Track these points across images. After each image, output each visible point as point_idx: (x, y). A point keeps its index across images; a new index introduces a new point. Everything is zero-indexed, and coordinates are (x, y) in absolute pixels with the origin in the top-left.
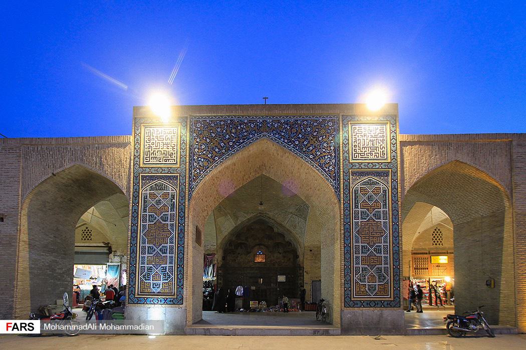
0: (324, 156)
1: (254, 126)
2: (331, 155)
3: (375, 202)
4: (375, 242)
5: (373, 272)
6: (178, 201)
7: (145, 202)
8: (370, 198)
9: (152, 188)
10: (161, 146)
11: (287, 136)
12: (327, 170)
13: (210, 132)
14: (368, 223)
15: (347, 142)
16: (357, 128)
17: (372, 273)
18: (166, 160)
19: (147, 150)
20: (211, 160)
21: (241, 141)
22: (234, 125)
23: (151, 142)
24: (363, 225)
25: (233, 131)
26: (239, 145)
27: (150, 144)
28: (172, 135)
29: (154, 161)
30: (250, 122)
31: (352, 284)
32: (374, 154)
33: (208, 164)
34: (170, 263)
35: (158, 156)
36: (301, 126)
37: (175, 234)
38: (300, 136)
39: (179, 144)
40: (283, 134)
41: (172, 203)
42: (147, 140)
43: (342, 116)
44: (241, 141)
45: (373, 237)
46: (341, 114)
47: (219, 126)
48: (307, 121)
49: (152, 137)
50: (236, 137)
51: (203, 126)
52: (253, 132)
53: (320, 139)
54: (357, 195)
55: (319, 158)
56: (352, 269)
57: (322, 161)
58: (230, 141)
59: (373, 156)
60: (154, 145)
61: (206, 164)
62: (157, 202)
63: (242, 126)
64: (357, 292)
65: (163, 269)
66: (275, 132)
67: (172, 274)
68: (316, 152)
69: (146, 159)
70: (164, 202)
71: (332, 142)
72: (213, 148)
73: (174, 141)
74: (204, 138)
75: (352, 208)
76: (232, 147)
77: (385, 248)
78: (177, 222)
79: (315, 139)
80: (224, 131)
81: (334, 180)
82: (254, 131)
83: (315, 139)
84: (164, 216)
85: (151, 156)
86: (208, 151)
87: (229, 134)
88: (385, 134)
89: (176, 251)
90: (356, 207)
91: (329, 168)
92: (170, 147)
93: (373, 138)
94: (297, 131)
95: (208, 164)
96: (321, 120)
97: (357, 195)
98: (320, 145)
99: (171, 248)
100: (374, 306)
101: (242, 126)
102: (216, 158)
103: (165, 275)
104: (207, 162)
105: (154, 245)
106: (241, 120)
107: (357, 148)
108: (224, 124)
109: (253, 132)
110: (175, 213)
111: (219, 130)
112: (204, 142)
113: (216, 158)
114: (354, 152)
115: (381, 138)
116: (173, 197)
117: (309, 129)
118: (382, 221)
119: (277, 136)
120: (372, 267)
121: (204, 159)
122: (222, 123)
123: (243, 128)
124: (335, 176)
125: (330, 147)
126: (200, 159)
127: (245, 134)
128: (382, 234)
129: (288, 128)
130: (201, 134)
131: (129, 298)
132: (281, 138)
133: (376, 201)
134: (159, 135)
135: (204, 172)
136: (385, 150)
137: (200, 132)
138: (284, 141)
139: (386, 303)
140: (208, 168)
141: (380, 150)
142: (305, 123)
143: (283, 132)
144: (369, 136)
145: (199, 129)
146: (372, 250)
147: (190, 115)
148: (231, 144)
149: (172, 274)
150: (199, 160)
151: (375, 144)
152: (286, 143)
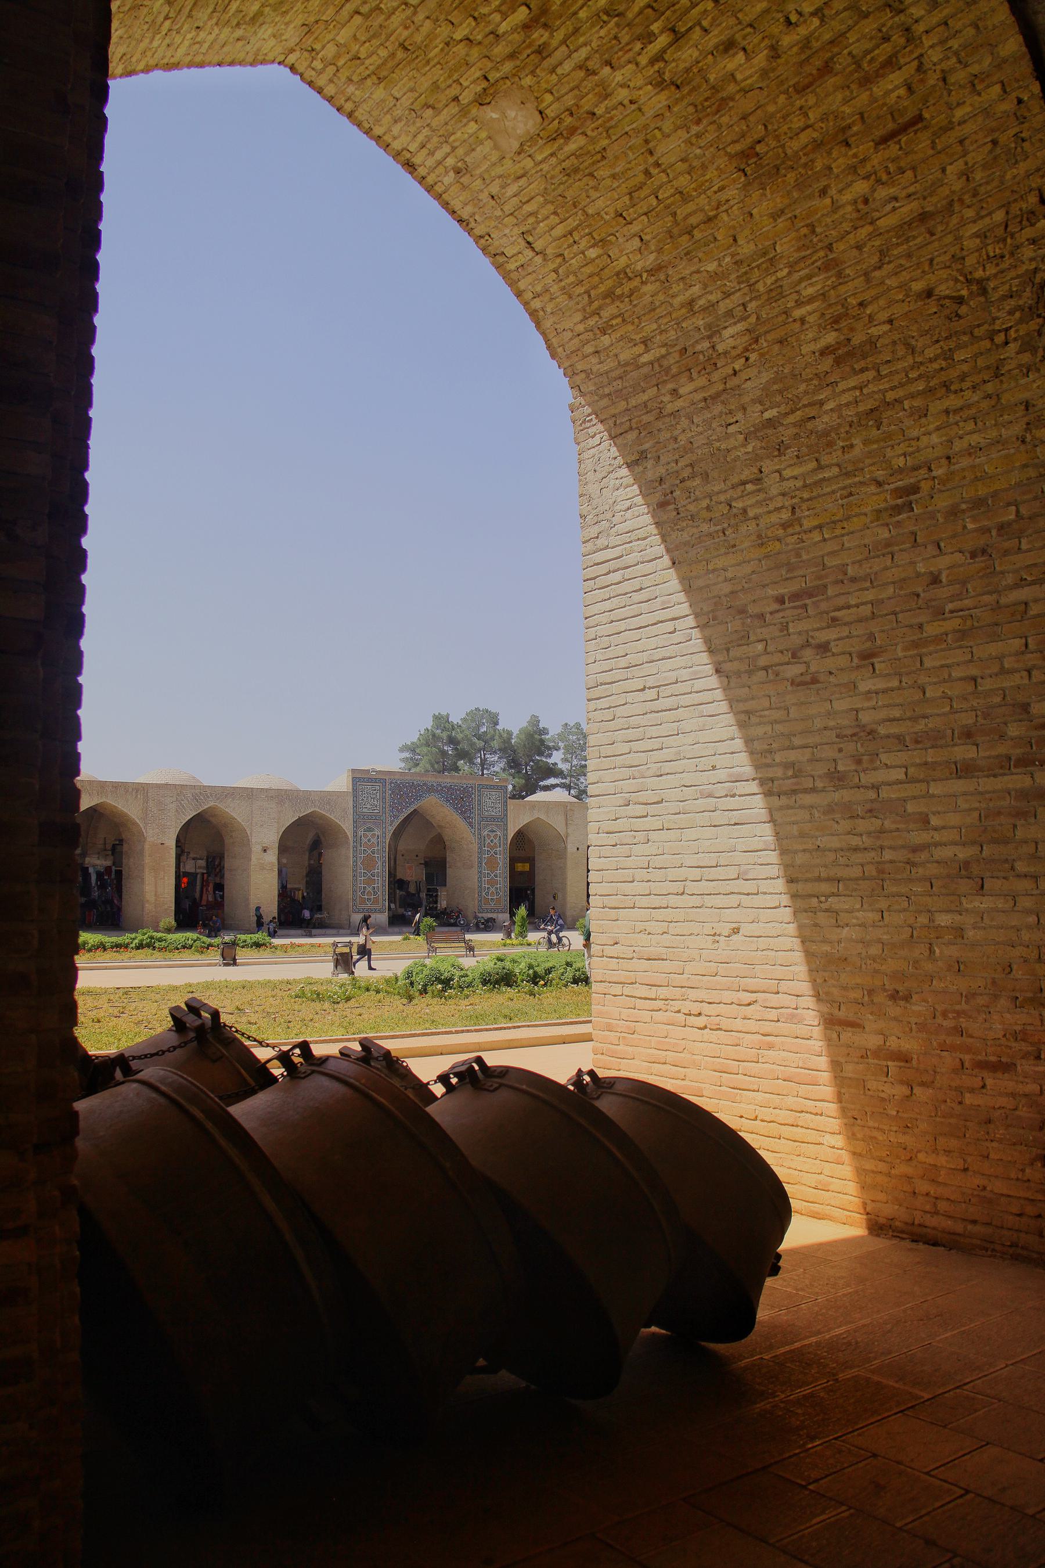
5: (493, 890)
8: (492, 841)
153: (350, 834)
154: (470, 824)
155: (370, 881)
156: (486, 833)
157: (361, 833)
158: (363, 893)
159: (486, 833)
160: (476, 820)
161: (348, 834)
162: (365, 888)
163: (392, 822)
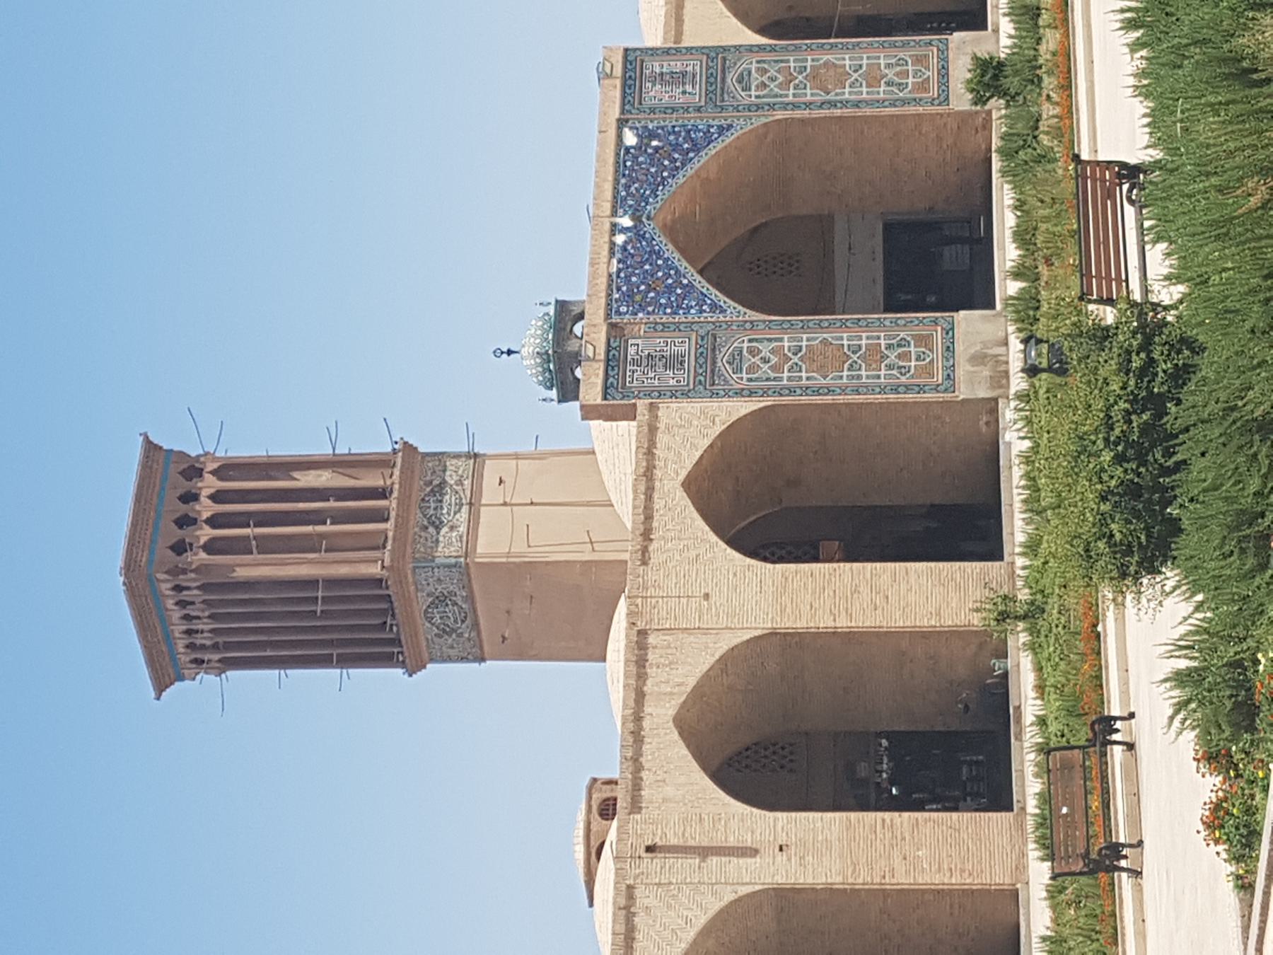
21: (657, 248)
70: (765, 353)
80: (637, 271)
102: (685, 282)
113: (685, 282)
117: (641, 159)
121: (684, 299)
123: (633, 247)
127: (644, 243)
129: (636, 185)
140: (702, 293)
148: (660, 262)
153: (744, 407)
154: (722, 130)
155: (874, 356)
158: (903, 370)
162: (889, 367)
163: (715, 307)
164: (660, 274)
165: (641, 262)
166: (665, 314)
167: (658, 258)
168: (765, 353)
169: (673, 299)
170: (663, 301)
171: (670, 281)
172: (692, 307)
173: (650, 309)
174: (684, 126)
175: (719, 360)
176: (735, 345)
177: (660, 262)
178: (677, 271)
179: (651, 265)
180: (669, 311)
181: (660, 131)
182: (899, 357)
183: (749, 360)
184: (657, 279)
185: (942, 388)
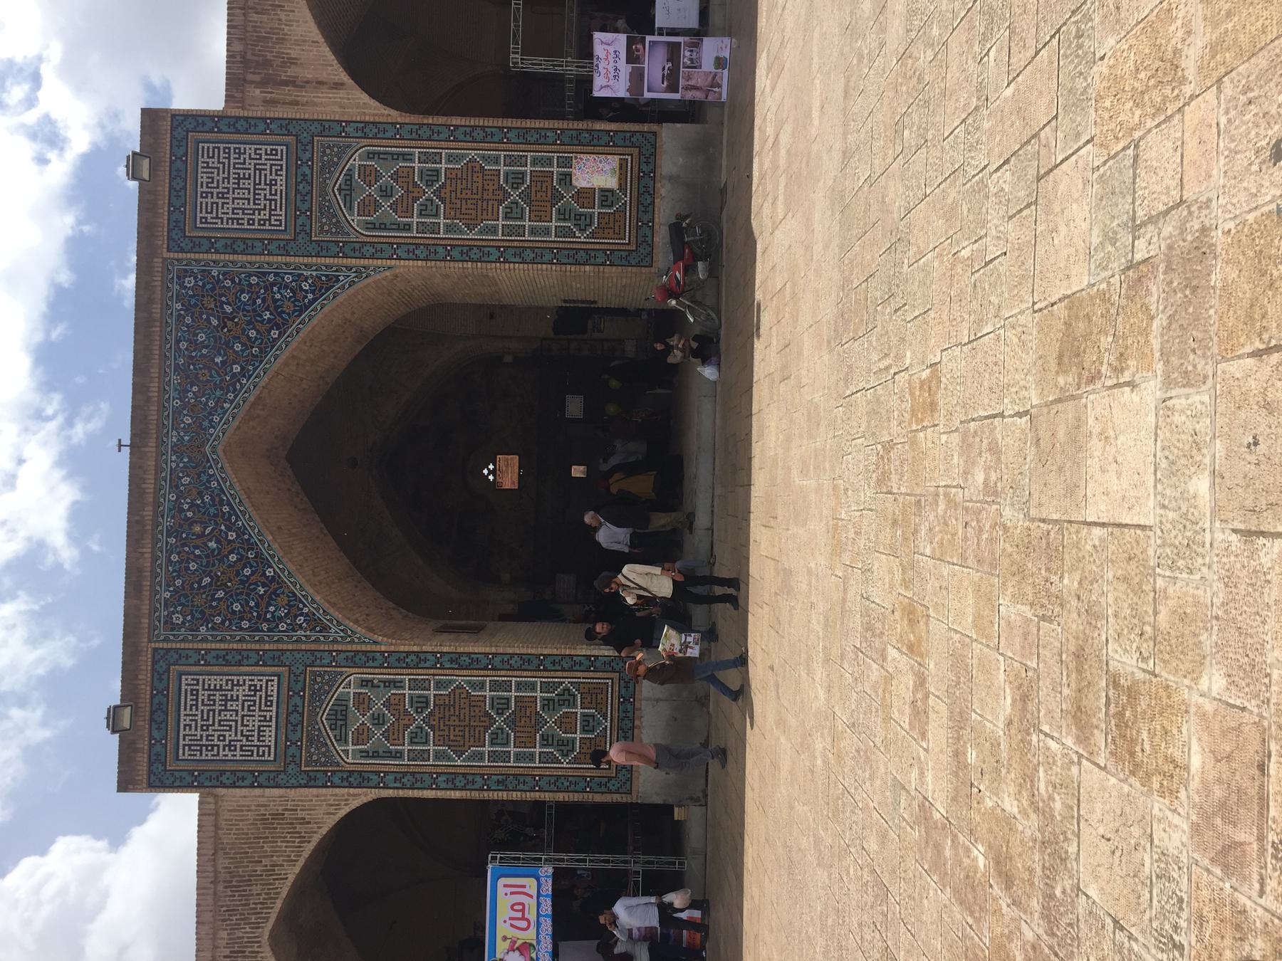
0: (275, 301)
1: (188, 476)
2: (273, 284)
3: (396, 181)
4: (496, 187)
6: (377, 671)
7: (376, 755)
8: (386, 192)
9: (342, 739)
10: (228, 717)
11: (218, 393)
12: (310, 296)
13: (200, 587)
14: (448, 201)
15: (239, 242)
16: (204, 214)
17: (572, 197)
18: (269, 703)
19: (238, 753)
20: (274, 586)
21: (226, 509)
22: (181, 526)
23: (216, 742)
24: (453, 213)
25: (197, 529)
26: (237, 516)
27: (221, 744)
28: (200, 687)
29: (270, 735)
30: (175, 486)
31: (597, 247)
32: (274, 177)
33: (283, 593)
34: (533, 689)
35: (257, 724)
36: (192, 357)
37: (461, 679)
38: (218, 360)
39: (226, 669)
40: (211, 403)
41: (382, 685)
42: (209, 753)
43: (169, 251)
44: (226, 509)
45: (483, 189)
46: (166, 255)
47: (183, 565)
48: (178, 341)
49: (204, 742)
50: (216, 523)
51: (179, 608)
52: (204, 478)
53: (228, 309)
54: (377, 226)
55: (280, 314)
56: (561, 246)
57: (288, 307)
58: (226, 539)
59: (279, 178)
60: (227, 734)
61: (283, 600)
62: (379, 724)
63: (186, 507)
64: (616, 236)
65: (548, 705)
66: (206, 423)
67: (562, 683)
68: (262, 322)
69: (263, 755)
71: (237, 280)
72: (242, 582)
73: (218, 683)
74: (214, 604)
75: (411, 237)
76: (241, 532)
77: (510, 161)
78: (432, 671)
79: (229, 323)
81: (338, 281)
82: (199, 476)
83: (229, 323)
84: (415, 705)
85: (256, 743)
86: (248, 595)
87: (205, 539)
88: (222, 146)
89: (503, 673)
90: (407, 227)
91: (306, 291)
92: (235, 693)
93: (232, 176)
94: (205, 367)
95: (283, 593)
96: (179, 306)
97: (377, 226)
98: (244, 310)
99: (495, 686)
100: (653, 196)
101: (186, 507)
102: (269, 572)
103: (564, 700)
104: (278, 595)
105: (486, 729)
106: (170, 510)
107: (256, 217)
108: (178, 553)
109: (204, 478)
110: (407, 678)
111: (193, 566)
112: (223, 606)
113: (269, 572)
114: (267, 227)
115: (233, 156)
116: (364, 683)
118: (444, 166)
119: (216, 419)
120: (557, 197)
121: (269, 605)
122: (174, 558)
123: (192, 505)
124: (326, 276)
125: (250, 285)
126: (269, 616)
128: (477, 169)
129: (195, 389)
130: (202, 613)
131: (617, 792)
132: (223, 408)
133: (396, 177)
134: (200, 723)
135: (306, 606)
136: (264, 147)
137: (198, 615)
138: (232, 402)
139: (644, 167)
140: (294, 595)
141: (263, 161)
142: (183, 345)
143: (206, 404)
144: (226, 185)
145: (189, 618)
146: (515, 195)
147: (150, 641)
149: (562, 683)
150: (273, 616)
151: (247, 172)
152: (235, 397)
156: (355, 219)
157: (349, 754)
159: (355, 219)
160: (312, 265)
161: (355, 804)
162: (546, 741)
164: (233, 558)
165: (202, 535)
166: (241, 629)
167: (229, 529)
168: (378, 706)
169: (252, 603)
170: (237, 607)
171: (247, 572)
172: (281, 619)
173: (218, 620)
174: (264, 274)
175: (319, 719)
176: (340, 689)
177: (232, 536)
178: (258, 555)
179: (218, 542)
180: (245, 624)
181: (228, 283)
182: (560, 723)
183: (359, 719)
184: (230, 566)
185: (614, 785)
